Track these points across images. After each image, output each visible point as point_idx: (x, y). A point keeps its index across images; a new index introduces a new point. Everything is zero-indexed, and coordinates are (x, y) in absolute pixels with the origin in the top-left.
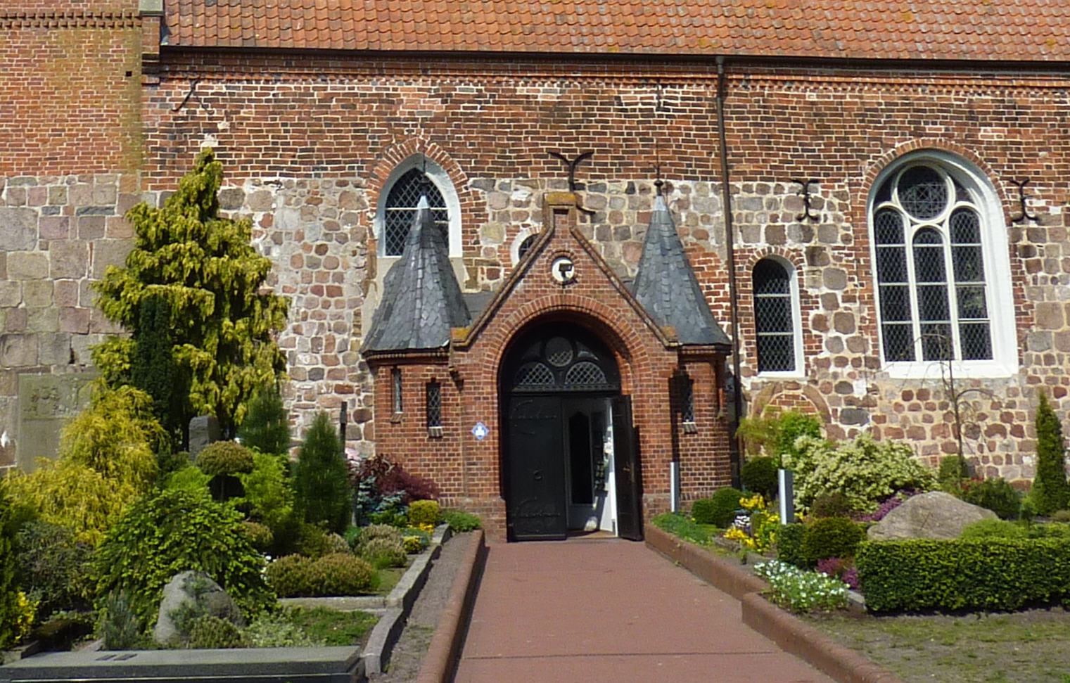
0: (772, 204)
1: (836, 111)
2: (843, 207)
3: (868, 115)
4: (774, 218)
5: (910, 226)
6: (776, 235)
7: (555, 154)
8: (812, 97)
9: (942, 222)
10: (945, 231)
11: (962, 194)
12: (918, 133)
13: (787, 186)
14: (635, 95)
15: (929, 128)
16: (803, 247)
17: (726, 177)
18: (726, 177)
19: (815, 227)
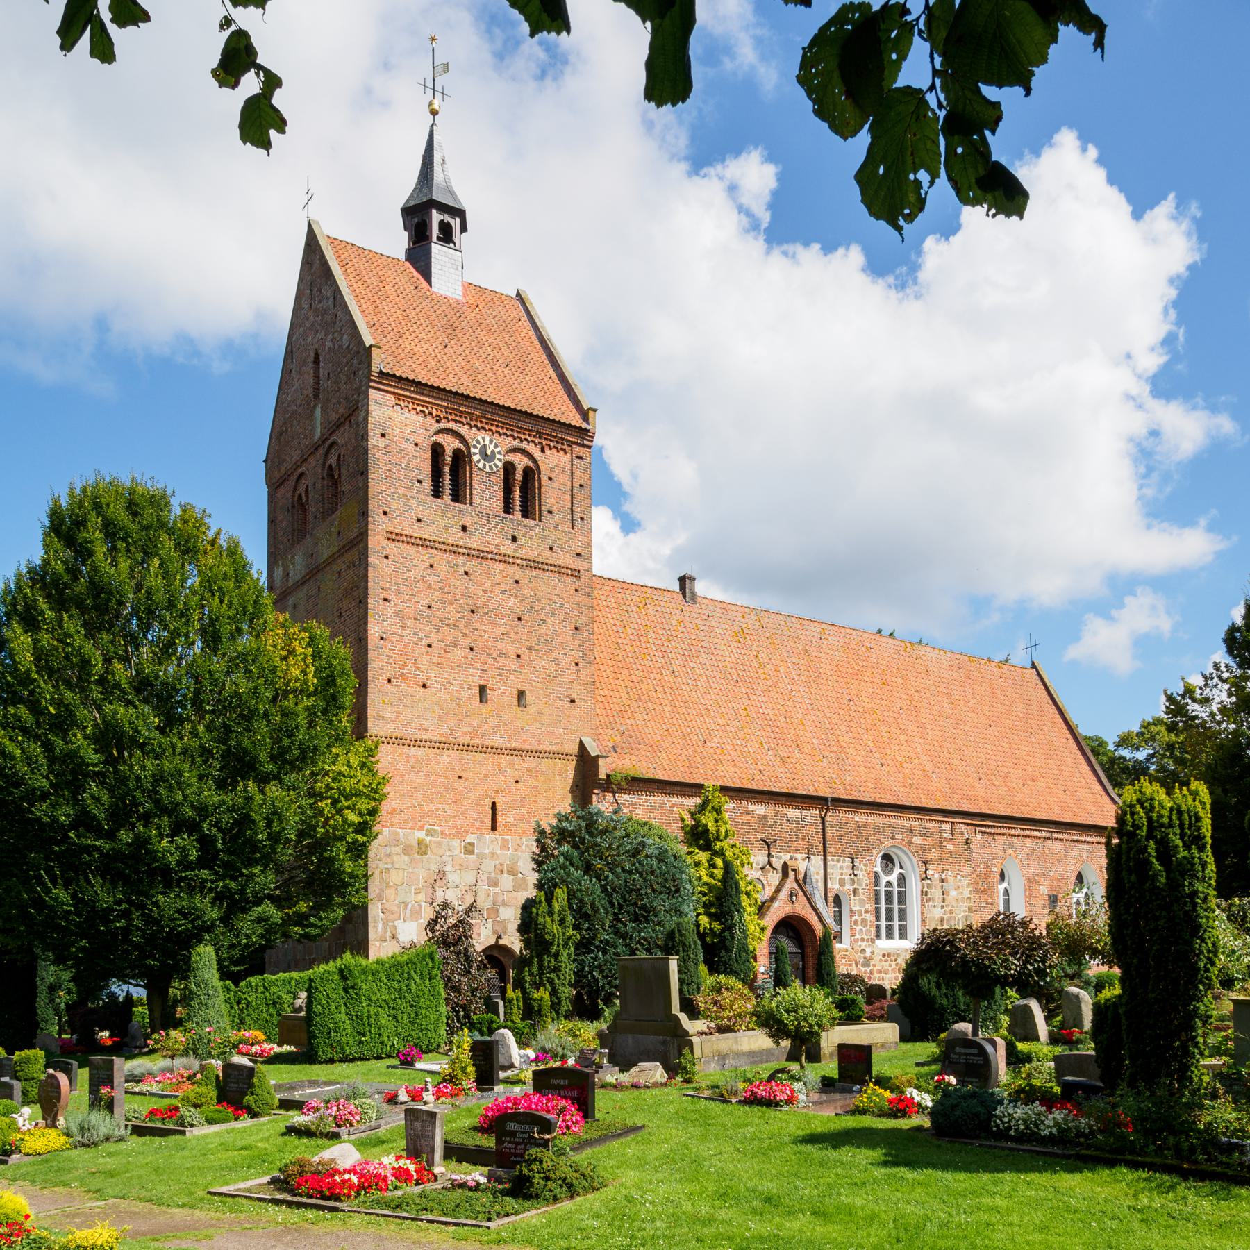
0: (841, 868)
1: (866, 825)
2: (866, 870)
3: (876, 828)
4: (842, 874)
5: (884, 879)
6: (842, 882)
7: (763, 841)
8: (857, 818)
9: (893, 878)
10: (895, 883)
11: (901, 867)
12: (893, 838)
13: (847, 859)
14: (793, 813)
15: (897, 836)
16: (852, 888)
17: (825, 855)
18: (825, 855)
19: (856, 879)
